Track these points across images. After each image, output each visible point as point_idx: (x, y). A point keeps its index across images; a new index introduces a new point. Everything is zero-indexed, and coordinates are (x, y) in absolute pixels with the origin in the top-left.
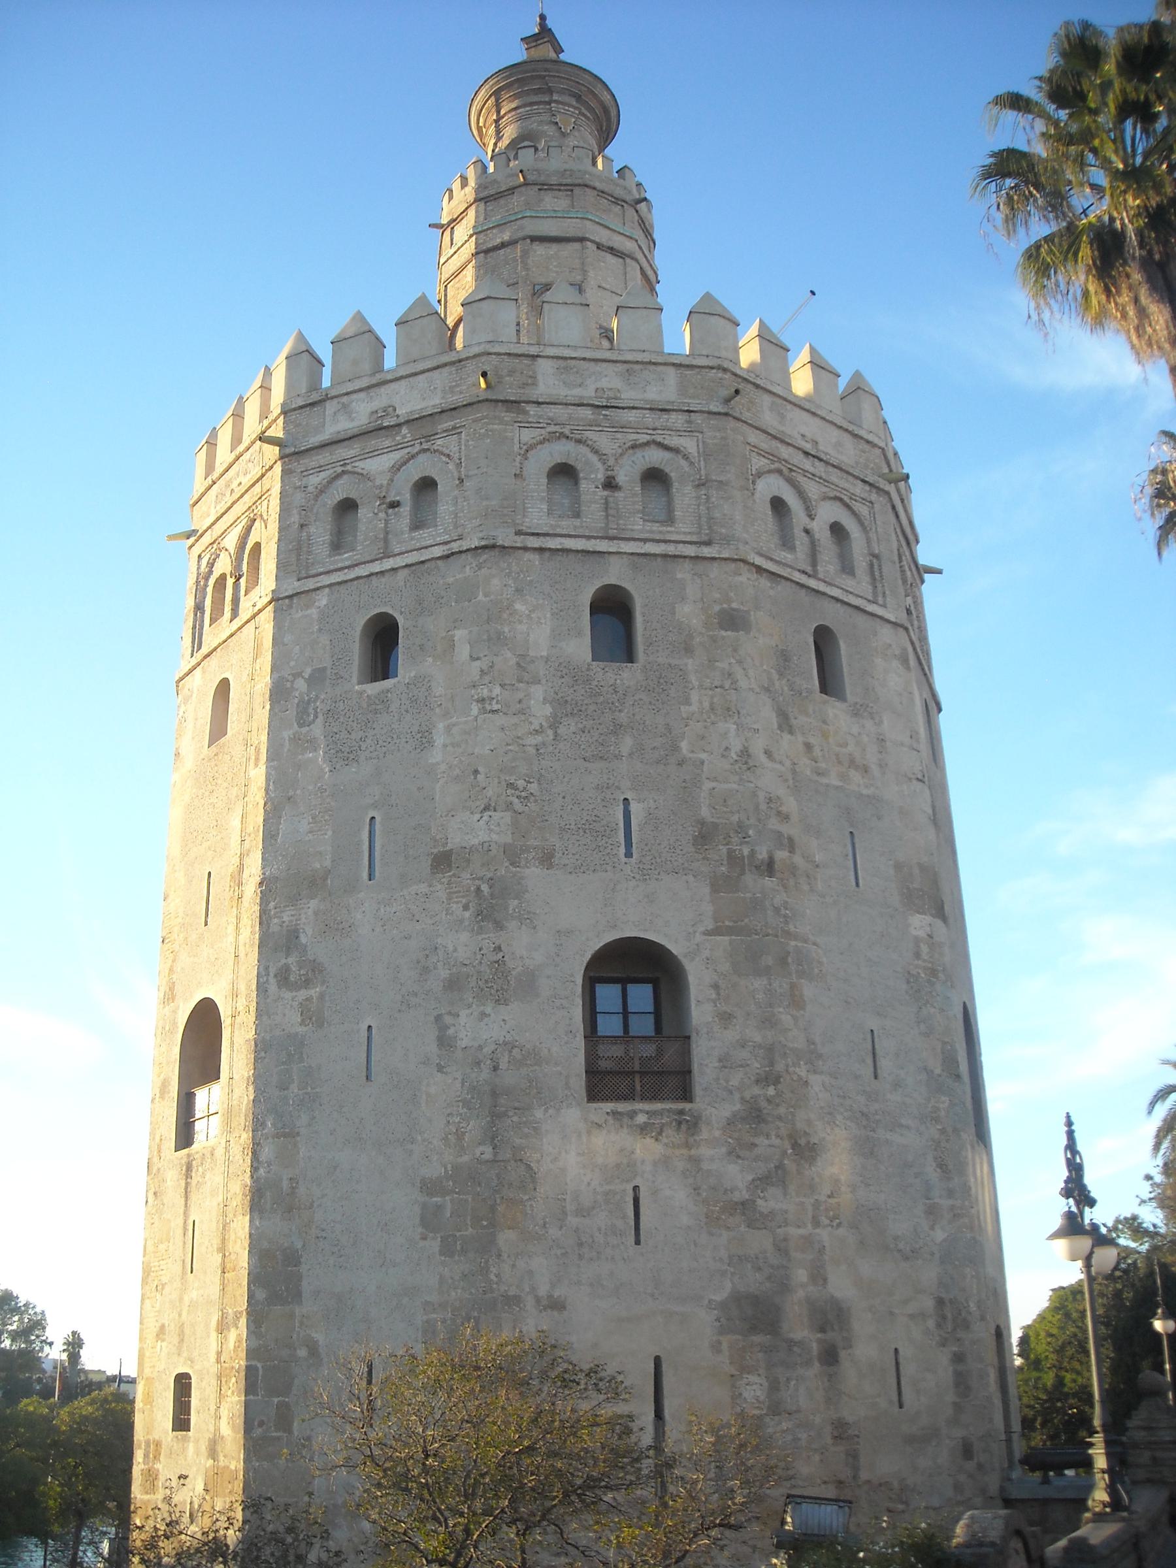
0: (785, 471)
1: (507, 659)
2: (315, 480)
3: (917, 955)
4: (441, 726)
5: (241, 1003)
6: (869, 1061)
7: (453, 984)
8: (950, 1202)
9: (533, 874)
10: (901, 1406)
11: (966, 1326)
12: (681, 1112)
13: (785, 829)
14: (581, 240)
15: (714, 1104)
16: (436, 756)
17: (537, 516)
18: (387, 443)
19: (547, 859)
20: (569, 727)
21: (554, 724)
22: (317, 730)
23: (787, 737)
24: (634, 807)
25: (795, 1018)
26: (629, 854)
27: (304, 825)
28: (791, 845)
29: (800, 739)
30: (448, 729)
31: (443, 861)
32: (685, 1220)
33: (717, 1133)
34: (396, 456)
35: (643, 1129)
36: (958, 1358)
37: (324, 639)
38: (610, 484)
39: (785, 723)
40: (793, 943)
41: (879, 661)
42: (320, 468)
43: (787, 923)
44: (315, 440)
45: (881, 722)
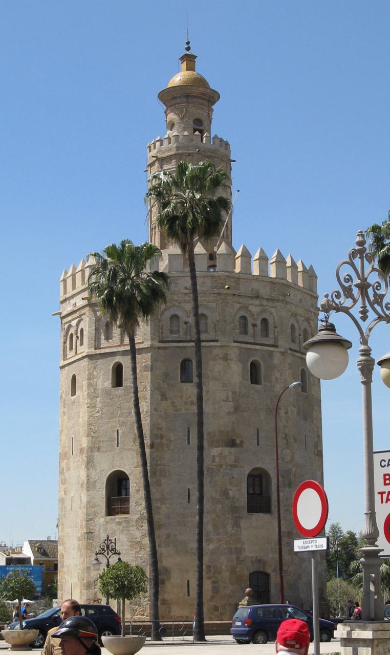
0: (177, 304)
3: (213, 461)
6: (187, 498)
8: (217, 537)
9: (96, 453)
10: (189, 595)
11: (220, 573)
12: (126, 518)
13: (159, 433)
16: (81, 420)
19: (99, 449)
21: (102, 409)
23: (164, 402)
24: (120, 431)
25: (157, 490)
26: (118, 446)
28: (162, 437)
29: (170, 401)
32: (126, 547)
33: (134, 523)
34: (76, 321)
36: (214, 582)
39: (164, 397)
40: (159, 467)
41: (211, 363)
43: (157, 462)
45: (209, 385)
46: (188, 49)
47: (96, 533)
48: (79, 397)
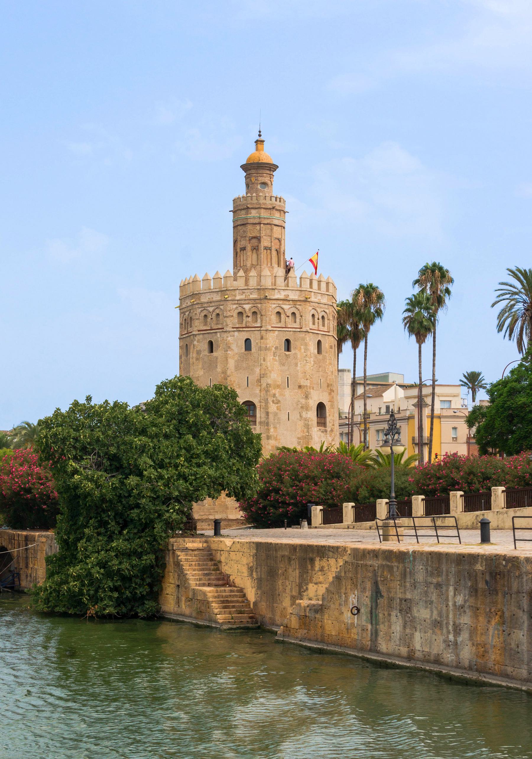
1: (309, 353)
2: (274, 306)
4: (299, 363)
5: (263, 404)
7: (302, 407)
9: (312, 390)
14: (282, 226)
15: (328, 429)
16: (298, 368)
17: (311, 326)
18: (288, 303)
20: (315, 365)
22: (277, 358)
27: (276, 375)
30: (301, 364)
31: (300, 387)
35: (322, 432)
37: (277, 341)
38: (318, 319)
42: (274, 304)
44: (274, 298)
46: (260, 136)
47: (313, 437)
48: (295, 354)
